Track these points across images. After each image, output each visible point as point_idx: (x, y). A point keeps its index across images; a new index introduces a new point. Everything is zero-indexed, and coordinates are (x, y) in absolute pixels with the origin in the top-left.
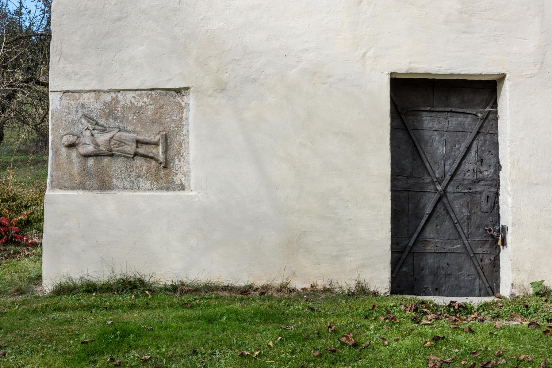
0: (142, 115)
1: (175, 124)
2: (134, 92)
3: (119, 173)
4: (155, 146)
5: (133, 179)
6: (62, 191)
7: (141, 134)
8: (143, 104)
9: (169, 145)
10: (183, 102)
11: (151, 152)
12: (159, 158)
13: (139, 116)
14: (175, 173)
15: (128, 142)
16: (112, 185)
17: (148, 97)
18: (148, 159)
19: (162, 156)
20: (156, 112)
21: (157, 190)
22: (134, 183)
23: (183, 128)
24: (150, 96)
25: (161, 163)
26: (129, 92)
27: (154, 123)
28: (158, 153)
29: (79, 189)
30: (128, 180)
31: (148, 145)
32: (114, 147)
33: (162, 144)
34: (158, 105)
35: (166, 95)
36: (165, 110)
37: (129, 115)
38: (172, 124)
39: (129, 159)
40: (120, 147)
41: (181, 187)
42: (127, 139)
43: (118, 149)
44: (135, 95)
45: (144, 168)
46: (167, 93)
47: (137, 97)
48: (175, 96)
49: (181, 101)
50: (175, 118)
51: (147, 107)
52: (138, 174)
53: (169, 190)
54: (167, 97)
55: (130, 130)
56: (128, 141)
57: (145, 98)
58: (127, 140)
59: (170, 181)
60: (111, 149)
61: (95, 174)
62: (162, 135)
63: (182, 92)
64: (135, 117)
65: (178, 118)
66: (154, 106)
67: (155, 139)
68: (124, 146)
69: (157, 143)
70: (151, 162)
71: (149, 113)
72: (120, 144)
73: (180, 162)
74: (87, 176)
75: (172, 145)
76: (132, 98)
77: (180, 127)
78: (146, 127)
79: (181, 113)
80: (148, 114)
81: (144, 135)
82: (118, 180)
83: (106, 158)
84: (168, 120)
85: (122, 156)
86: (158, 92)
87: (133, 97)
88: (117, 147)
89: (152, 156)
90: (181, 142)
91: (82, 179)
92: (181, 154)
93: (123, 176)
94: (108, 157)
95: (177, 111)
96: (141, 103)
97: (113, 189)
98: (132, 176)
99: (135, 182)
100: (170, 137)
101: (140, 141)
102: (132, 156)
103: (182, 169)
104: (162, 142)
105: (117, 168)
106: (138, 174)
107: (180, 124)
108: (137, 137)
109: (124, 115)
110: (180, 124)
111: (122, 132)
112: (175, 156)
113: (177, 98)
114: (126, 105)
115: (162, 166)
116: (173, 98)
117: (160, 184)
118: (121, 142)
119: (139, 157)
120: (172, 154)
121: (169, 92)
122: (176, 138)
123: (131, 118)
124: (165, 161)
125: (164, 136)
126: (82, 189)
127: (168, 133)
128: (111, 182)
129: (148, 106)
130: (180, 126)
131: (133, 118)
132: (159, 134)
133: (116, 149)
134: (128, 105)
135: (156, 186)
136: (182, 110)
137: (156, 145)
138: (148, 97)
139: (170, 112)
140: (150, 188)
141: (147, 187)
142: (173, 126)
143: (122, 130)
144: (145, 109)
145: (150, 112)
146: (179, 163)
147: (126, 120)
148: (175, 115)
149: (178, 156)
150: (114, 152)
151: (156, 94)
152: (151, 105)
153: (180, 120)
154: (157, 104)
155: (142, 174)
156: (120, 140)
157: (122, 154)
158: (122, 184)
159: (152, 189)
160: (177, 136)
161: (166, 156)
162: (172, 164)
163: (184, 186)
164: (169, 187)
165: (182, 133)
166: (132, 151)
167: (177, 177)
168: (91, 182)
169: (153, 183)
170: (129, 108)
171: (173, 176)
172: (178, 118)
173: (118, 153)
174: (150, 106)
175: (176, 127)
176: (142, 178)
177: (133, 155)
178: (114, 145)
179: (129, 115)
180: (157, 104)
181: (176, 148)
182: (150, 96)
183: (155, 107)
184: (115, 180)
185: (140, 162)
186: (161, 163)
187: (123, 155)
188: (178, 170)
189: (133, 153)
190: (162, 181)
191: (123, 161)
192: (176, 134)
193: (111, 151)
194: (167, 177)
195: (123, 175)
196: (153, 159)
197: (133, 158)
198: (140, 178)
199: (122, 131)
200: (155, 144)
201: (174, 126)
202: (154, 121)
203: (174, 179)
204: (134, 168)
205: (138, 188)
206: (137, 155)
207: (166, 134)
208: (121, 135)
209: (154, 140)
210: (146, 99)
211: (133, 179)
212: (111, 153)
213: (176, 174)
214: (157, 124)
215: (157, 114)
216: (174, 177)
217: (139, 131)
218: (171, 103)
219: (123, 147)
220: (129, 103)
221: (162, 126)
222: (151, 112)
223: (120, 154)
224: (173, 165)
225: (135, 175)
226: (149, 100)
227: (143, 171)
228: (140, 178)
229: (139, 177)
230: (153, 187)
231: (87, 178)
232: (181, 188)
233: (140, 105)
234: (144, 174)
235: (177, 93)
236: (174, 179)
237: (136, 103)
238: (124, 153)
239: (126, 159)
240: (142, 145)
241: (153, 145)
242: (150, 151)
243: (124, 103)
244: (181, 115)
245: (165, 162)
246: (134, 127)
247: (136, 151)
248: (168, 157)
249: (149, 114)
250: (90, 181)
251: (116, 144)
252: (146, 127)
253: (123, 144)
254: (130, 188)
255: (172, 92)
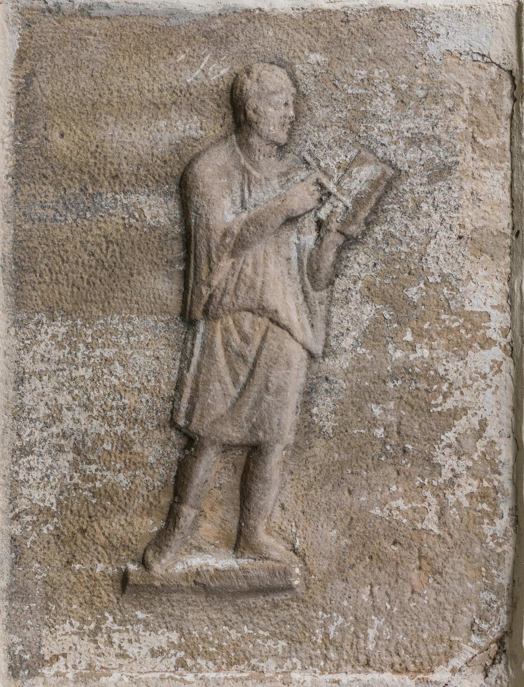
0: (390, 470)
1: (341, 630)
2: (507, 430)
3: (98, 352)
4: (235, 531)
5: (68, 423)
6: (11, 64)
7: (291, 466)
8: (447, 474)
9: (239, 602)
10: (453, 671)
11: (201, 514)
12: (169, 555)
13: (386, 453)
14: (98, 628)
15: (250, 403)
16: (37, 317)
17: (483, 496)
18: (165, 500)
19: (179, 568)
20: (402, 540)
21: (13, 539)
22: (47, 426)
23: (323, 671)
24: (485, 506)
25: (144, 563)
26: (510, 403)
27: (350, 526)
28: (199, 549)
29: (17, 151)
30: (64, 399)
31: (237, 501)
32: (226, 329)
33: (243, 569)
34: (440, 548)
35: (490, 588)
36: (416, 583)
37: (391, 405)
38: (341, 619)
39: (169, 405)
40: (229, 363)
41: (27, 657)
42: (269, 398)
43: (219, 350)
44: (491, 432)
45: (121, 476)
46: (497, 594)
47: (481, 445)
48: (481, 633)
49: (455, 662)
50: (372, 633)
51: (428, 494)
52: (93, 450)
53: (11, 600)
54: (481, 590)
55: (315, 410)
56: (258, 403)
57: (476, 483)
58: (261, 399)
59: (55, 602)
60: (216, 318)
61: (96, 231)
62: (286, 573)
63: (499, 669)
64: (379, 432)
65: (371, 647)
66: (436, 531)
67: (268, 532)
68: (235, 381)
69: (247, 542)
70: (149, 514)
71: (400, 503)
72: (245, 361)
73: (154, 653)
74: (84, 190)
75: (234, 617)
76: (475, 421)
77: (326, 658)
78: (329, 487)
79: (396, 659)
80: (394, 499)
81: (288, 477)
82: (60, 346)
83: (175, 287)
84: (365, 597)
85: (181, 369)
86: (506, 547)
87: (483, 424)
88: (227, 345)
89: (182, 522)
90: (253, 661)
91: (71, 166)
92: (190, 662)
93: (82, 372)
94: (180, 298)
95: (406, 641)
96: (453, 462)
97: (19, 324)
98: (83, 417)
99: (54, 430)
100: (276, 606)
101: (255, 463)
102: (182, 422)
103: (115, 662)
104: (253, 574)
105: (123, 341)
106: (93, 450)
107: (341, 658)
108: (279, 448)
109: (393, 377)
110: (341, 658)
111: (304, 370)
112: (180, 630)
113: (474, 638)
114: (445, 387)
115: (132, 567)
116: (473, 623)
117: (40, 557)
118: (254, 365)
119: (175, 455)
120: (191, 616)
121: (505, 600)
122: (273, 635)
123: (377, 411)
124: (157, 583)
125: (279, 582)
126: (18, 165)
127: (298, 599)
128: (51, 311)
129: (433, 500)
130: (332, 655)
131: (374, 423)
132: (295, 551)
133: (218, 339)
134: (445, 397)
135: (33, 536)
136: (412, 667)
137: (238, 539)
138: (483, 496)
139: (403, 610)
140: (23, 504)
141: (25, 491)
142: (331, 620)
143: (315, 367)
144: (422, 486)
145: (403, 507)
146: (145, 650)
147: (367, 390)
148: (387, 630)
149: (179, 647)
150: (201, 327)
151: (494, 536)
152: (441, 514)
153: (362, 658)
154: (444, 541)
155: (93, 467)
156: (262, 360)
157: (192, 368)
158: (41, 366)
159: (17, 517)
160: (283, 643)
161: (179, 589)
162: (141, 615)
163: (31, 675)
164: (26, 600)
165: (294, 668)
166: (208, 421)
167: (76, 638)
168: (51, 213)
169: (46, 522)
170: (428, 404)
171: (83, 621)
172: (371, 647)
173: (197, 351)
174: (435, 508)
175: (326, 635)
176: (74, 465)
177: (187, 427)
178: (240, 332)
179: (391, 405)
180: (444, 541)
181: (220, 636)
182: (485, 506)
183: (429, 532)
184: (63, 330)
185: (151, 459)
186: (144, 563)
187: (189, 378)
188: (111, 643)
189: (195, 426)
190: (57, 563)
191: (157, 374)
192: (290, 639)
193: (206, 312)
194: (79, 588)
195: (89, 374)
196: (167, 522)
197: (173, 423)
198: (71, 456)
199: (309, 368)
200: (240, 532)
201: (332, 629)
202: (359, 528)
203: (67, 626)
204: (121, 428)
205: (22, 449)
206: (187, 447)
207: (290, 588)
208: (288, 365)
209: (261, 529)
210: (469, 489)
211: (68, 423)
212: (198, 313)
213: (94, 634)
214: (345, 541)
215: (395, 543)
216: (77, 624)
217: (308, 453)
218: (447, 614)
219: (228, 379)
220: (450, 404)
221: (334, 568)
222: (405, 514)
223: (195, 361)
224: (139, 621)
225: (86, 433)
226: (466, 503)
227: (109, 474)
228: (71, 456)
229: (77, 450)
230: (29, 518)
231: (76, 189)
232: (22, 661)
233: (439, 458)
234: (93, 479)
235: (500, 642)
236: (67, 626)
237: (450, 436)
238: (196, 382)
239: (167, 390)
240: (240, 472)
241: (236, 522)
242: (207, 510)
243: (452, 376)
244: (387, 659)
245: (152, 586)
246: (329, 426)
247: (207, 443)
248: (175, 597)
249: (394, 504)
250: (60, 207)
251: (245, 339)
252: (329, 487)
253: (242, 379)
254: (22, 407)
255: (503, 618)
